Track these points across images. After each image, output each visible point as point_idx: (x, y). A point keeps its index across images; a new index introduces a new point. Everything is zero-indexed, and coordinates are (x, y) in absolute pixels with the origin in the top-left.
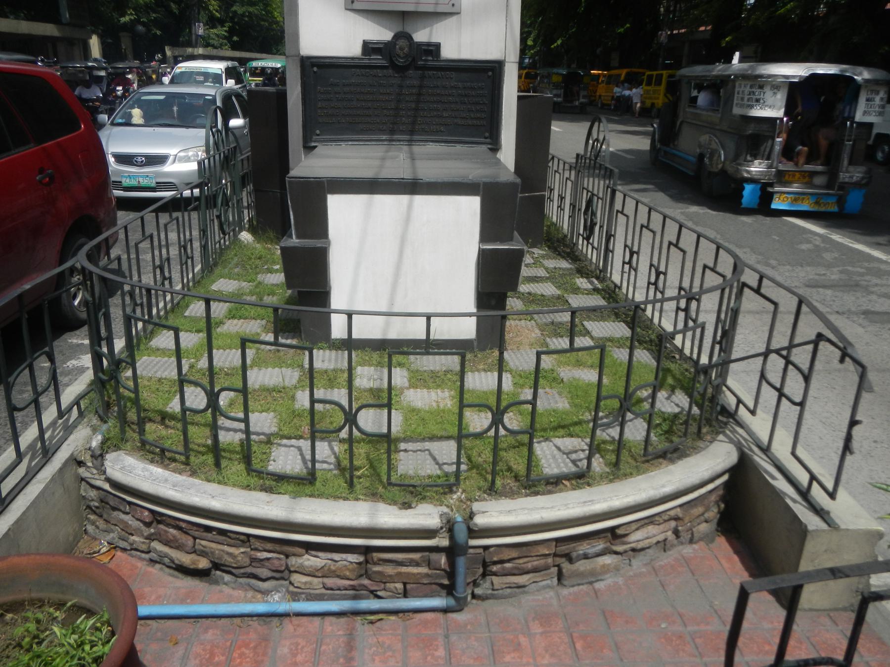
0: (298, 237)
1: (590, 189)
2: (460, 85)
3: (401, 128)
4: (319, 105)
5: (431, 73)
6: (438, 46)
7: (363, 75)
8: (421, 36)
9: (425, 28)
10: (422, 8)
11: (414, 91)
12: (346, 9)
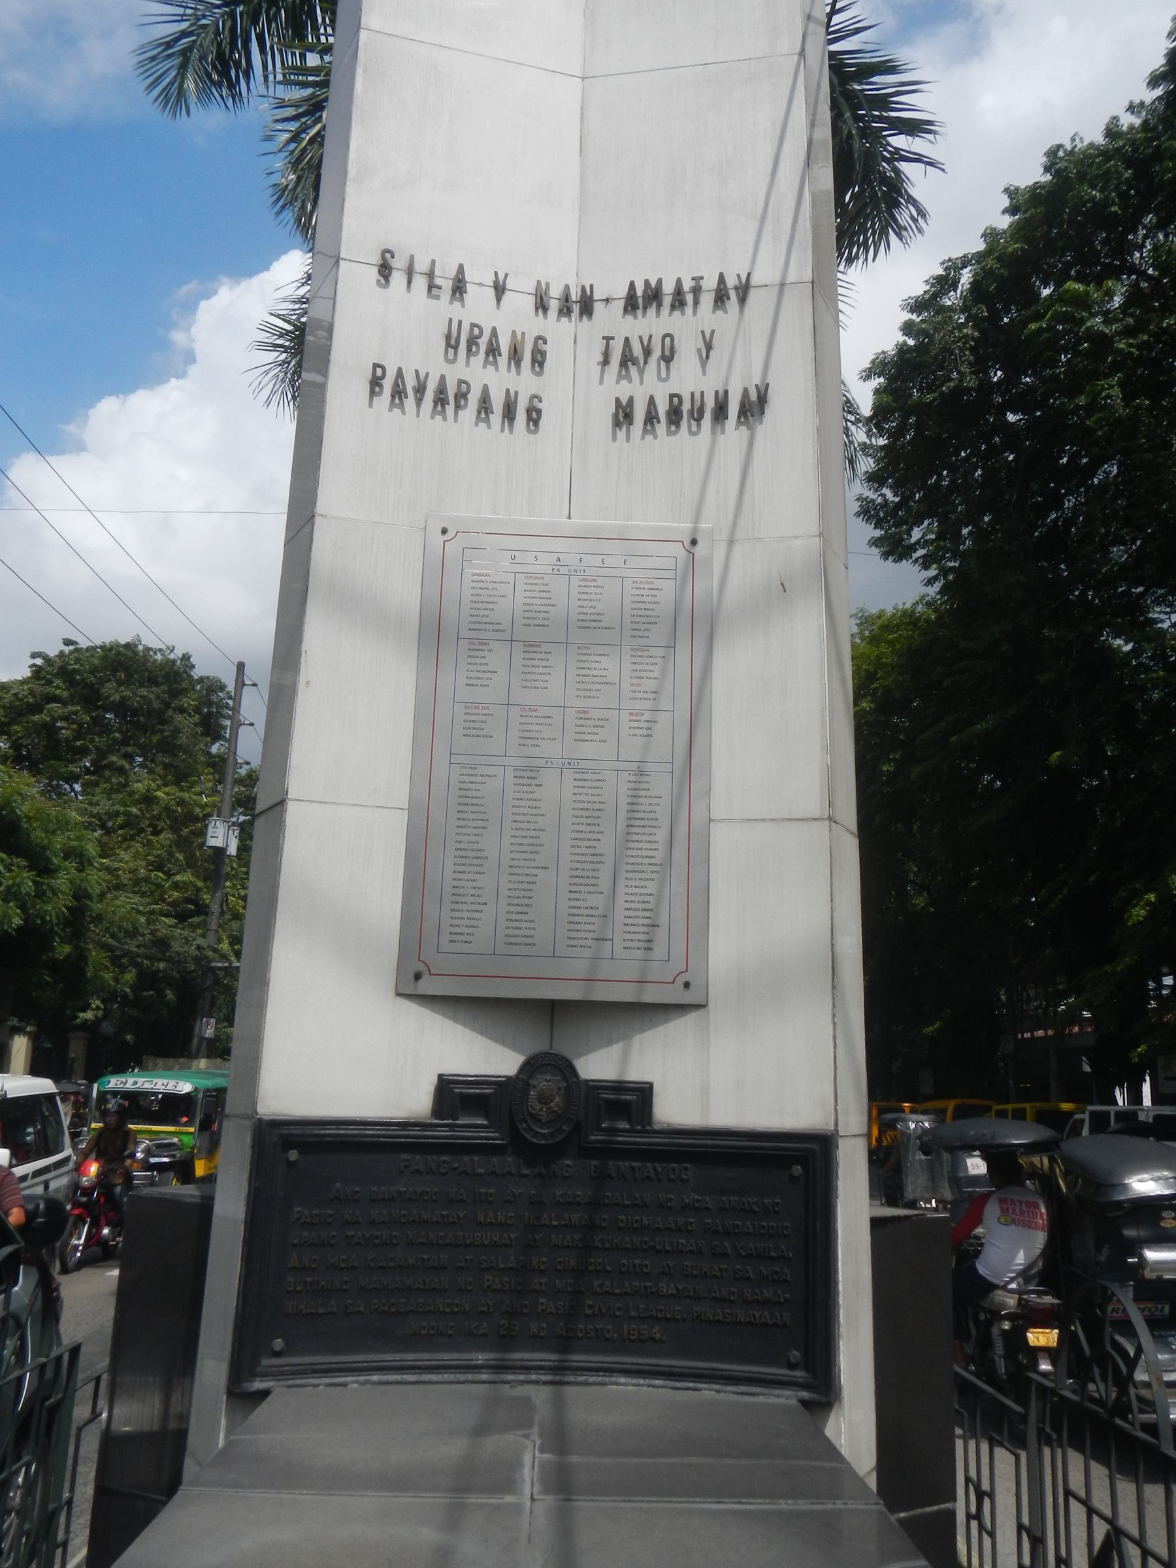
1: (1104, 1506)
3: (534, 1327)
5: (624, 1165)
6: (645, 1092)
8: (597, 1065)
9: (609, 1042)
12: (398, 994)
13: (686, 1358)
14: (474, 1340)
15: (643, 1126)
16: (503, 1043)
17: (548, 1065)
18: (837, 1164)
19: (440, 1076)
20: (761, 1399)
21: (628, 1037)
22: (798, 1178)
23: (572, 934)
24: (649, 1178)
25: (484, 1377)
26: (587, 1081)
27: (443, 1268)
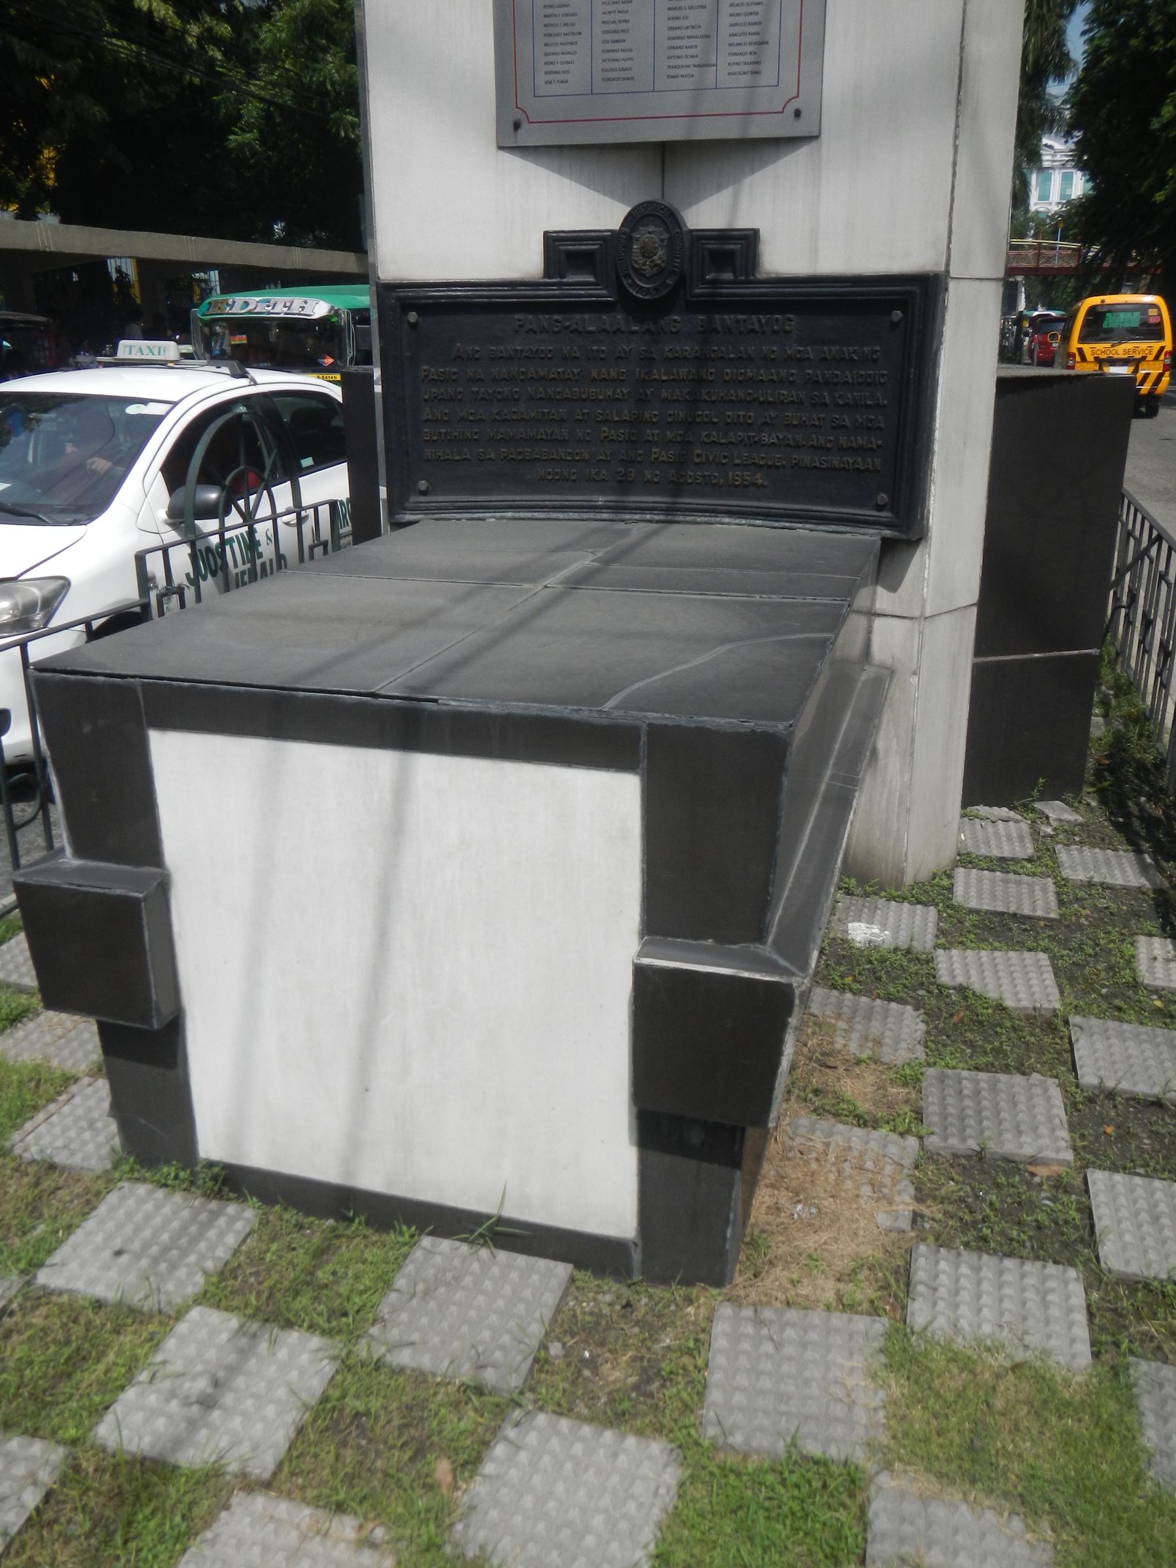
0: (79, 852)
2: (811, 352)
4: (427, 413)
5: (729, 318)
6: (750, 240)
7: (544, 331)
8: (706, 214)
9: (719, 188)
10: (706, 131)
11: (683, 371)
12: (500, 148)
13: (785, 501)
14: (597, 484)
15: (747, 276)
16: (612, 196)
17: (652, 215)
18: (945, 308)
19: (546, 234)
20: (848, 536)
21: (737, 180)
22: (898, 324)
23: (673, 62)
24: (753, 330)
25: (605, 516)
26: (691, 231)
27: (562, 420)
